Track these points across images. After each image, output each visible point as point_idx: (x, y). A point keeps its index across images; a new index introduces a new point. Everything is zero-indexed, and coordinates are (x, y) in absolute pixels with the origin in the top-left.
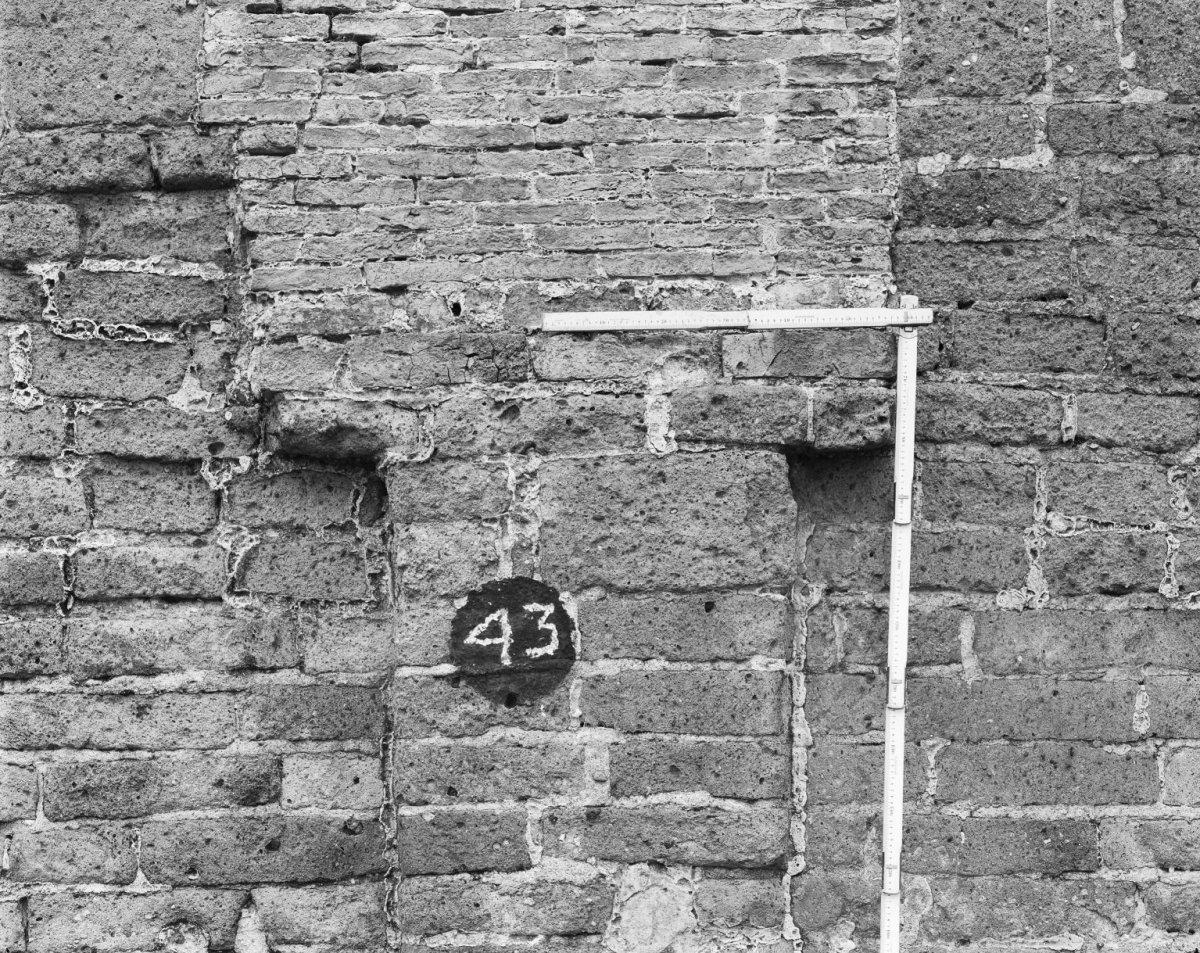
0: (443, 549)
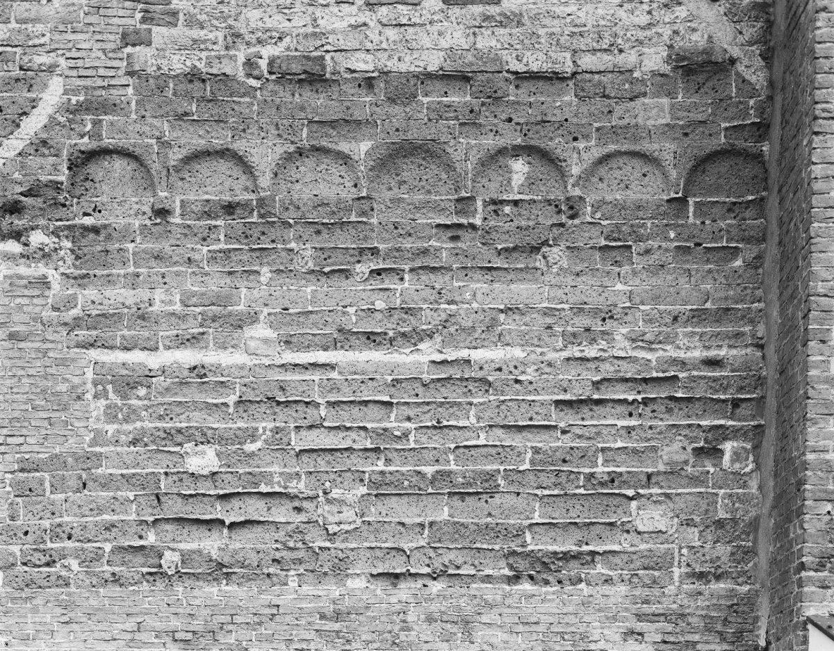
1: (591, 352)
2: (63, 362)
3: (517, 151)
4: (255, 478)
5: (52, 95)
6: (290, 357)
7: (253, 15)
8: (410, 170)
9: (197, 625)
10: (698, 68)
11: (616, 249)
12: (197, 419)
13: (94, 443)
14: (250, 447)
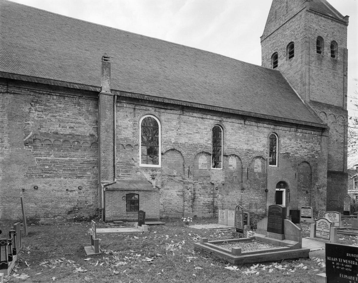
0: (215, 186)
1: (83, 159)
2: (33, 158)
3: (76, 141)
4: (52, 169)
5: (31, 133)
6: (55, 158)
7: (51, 128)
8: (66, 142)
9: (47, 182)
10: (92, 135)
11: (85, 150)
12: (46, 164)
14: (52, 166)
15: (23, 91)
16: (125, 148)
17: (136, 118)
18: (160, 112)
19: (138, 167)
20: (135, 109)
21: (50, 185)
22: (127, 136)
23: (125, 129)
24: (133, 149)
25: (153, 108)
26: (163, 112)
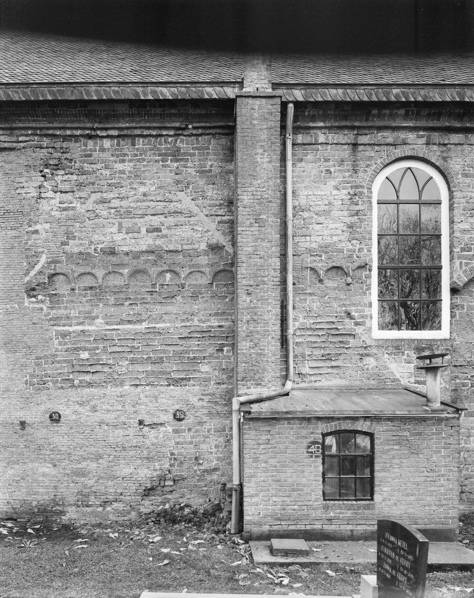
1: (188, 324)
2: (47, 330)
3: (167, 271)
4: (98, 360)
5: (43, 259)
6: (108, 327)
7: (96, 236)
8: (139, 277)
9: (84, 399)
10: (215, 248)
11: (195, 296)
12: (83, 345)
13: (55, 351)
14: (97, 352)
15: (21, 139)
16: (321, 281)
17: (361, 174)
18: (445, 145)
19: (369, 342)
20: (355, 145)
21: (94, 409)
22: (329, 240)
23: (324, 215)
24: (349, 280)
25: (421, 133)
26: (459, 144)
